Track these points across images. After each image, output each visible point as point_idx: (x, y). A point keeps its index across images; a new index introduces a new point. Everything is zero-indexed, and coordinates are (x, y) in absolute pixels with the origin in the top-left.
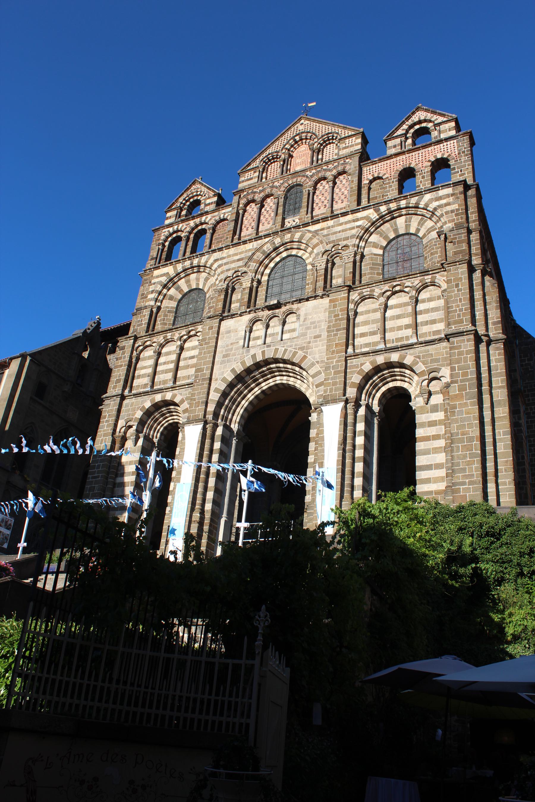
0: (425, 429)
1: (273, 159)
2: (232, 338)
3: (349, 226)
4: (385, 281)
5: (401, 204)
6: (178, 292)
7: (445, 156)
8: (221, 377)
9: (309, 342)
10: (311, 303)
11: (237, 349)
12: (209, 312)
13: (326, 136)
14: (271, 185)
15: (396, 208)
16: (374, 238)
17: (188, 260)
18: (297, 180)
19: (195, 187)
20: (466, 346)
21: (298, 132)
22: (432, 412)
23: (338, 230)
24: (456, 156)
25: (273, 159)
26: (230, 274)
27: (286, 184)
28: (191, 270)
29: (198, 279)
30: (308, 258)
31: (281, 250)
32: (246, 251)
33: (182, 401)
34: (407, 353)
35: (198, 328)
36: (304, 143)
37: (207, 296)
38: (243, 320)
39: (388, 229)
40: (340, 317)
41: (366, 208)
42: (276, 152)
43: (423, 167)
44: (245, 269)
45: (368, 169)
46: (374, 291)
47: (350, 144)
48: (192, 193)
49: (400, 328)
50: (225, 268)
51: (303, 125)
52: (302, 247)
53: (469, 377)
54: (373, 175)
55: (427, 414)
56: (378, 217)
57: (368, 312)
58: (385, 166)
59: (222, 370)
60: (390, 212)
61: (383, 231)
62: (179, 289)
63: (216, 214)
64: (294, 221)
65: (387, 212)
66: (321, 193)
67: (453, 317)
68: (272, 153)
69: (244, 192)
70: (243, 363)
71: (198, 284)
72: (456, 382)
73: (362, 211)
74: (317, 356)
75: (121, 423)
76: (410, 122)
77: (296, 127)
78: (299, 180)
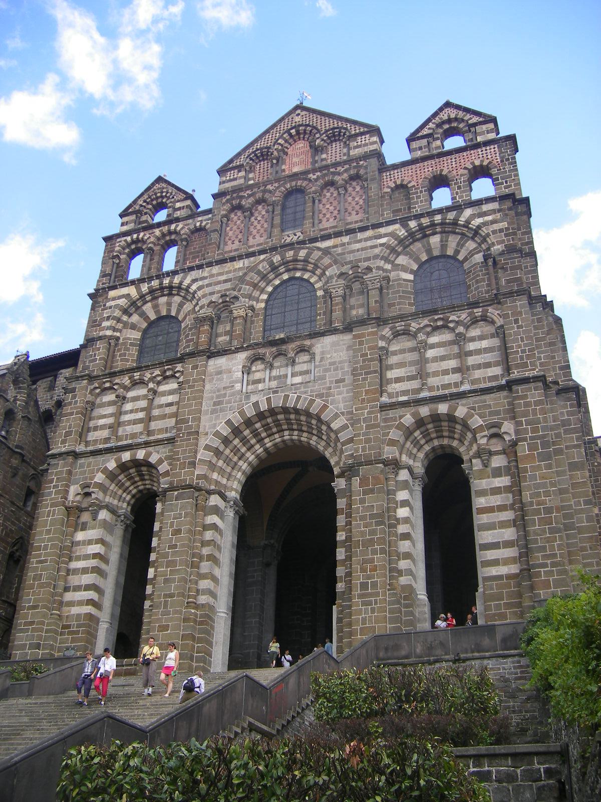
0: (486, 497)
2: (225, 380)
3: (369, 243)
4: (425, 313)
5: (435, 219)
7: (485, 163)
8: (212, 430)
9: (330, 388)
10: (328, 340)
11: (233, 394)
12: (188, 346)
14: (262, 188)
16: (402, 260)
17: (156, 279)
18: (296, 183)
19: (160, 186)
20: (533, 396)
21: (293, 125)
22: (494, 476)
23: (356, 248)
24: (499, 164)
26: (214, 298)
27: (282, 188)
29: (169, 304)
30: (316, 282)
32: (235, 270)
33: (160, 461)
34: (458, 404)
35: (177, 367)
36: (302, 139)
37: (183, 325)
38: (238, 358)
39: (419, 249)
40: (369, 357)
42: (266, 148)
43: (458, 175)
44: (236, 293)
45: (388, 174)
46: (410, 325)
47: (363, 142)
48: (156, 194)
49: (446, 372)
50: (207, 290)
52: (308, 268)
53: (541, 433)
54: (395, 182)
55: (489, 480)
57: (402, 351)
58: (410, 171)
60: (421, 228)
62: (143, 315)
63: (190, 221)
64: (296, 235)
66: (328, 201)
67: (515, 359)
68: (261, 149)
69: (226, 195)
70: (242, 413)
71: (169, 310)
72: (525, 439)
73: (386, 226)
75: (73, 489)
77: (290, 117)
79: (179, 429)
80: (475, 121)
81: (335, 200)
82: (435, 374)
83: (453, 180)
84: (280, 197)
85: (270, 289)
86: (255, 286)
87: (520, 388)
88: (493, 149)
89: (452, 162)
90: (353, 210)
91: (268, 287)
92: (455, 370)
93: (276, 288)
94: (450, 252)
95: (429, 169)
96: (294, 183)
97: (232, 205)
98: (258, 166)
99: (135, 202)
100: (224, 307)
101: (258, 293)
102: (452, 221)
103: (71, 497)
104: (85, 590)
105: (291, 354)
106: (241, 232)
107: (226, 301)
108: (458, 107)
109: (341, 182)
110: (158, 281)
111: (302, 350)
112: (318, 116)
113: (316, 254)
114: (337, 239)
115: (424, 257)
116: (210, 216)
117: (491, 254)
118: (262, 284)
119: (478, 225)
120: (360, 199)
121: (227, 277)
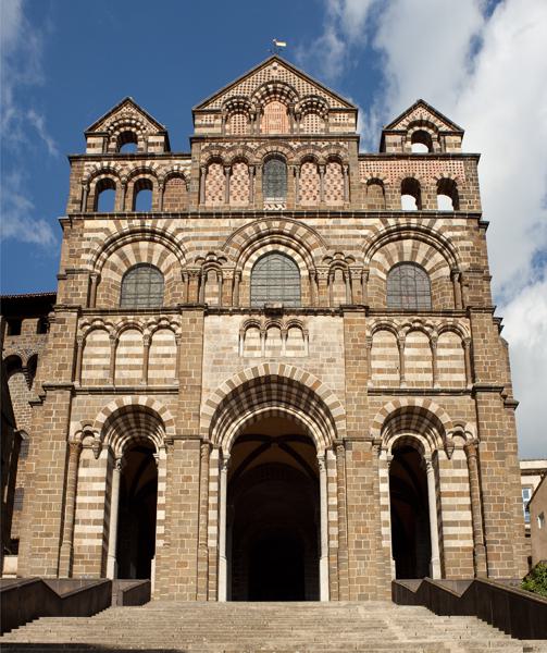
1: (238, 107)
3: (352, 232)
4: (408, 312)
6: (121, 262)
7: (453, 178)
9: (322, 366)
11: (232, 356)
16: (378, 257)
26: (202, 254)
29: (151, 251)
32: (221, 229)
33: (163, 410)
39: (393, 250)
42: (243, 98)
44: (222, 253)
49: (419, 371)
54: (371, 175)
57: (383, 345)
59: (215, 380)
62: (123, 256)
63: (167, 162)
70: (242, 375)
71: (150, 258)
72: (485, 440)
74: (333, 383)
75: (75, 426)
76: (410, 118)
79: (182, 381)
82: (411, 370)
87: (483, 394)
88: (459, 164)
92: (427, 370)
95: (402, 169)
96: (275, 148)
103: (72, 433)
104: (94, 524)
105: (284, 328)
107: (213, 261)
108: (430, 110)
110: (139, 221)
111: (294, 325)
116: (189, 161)
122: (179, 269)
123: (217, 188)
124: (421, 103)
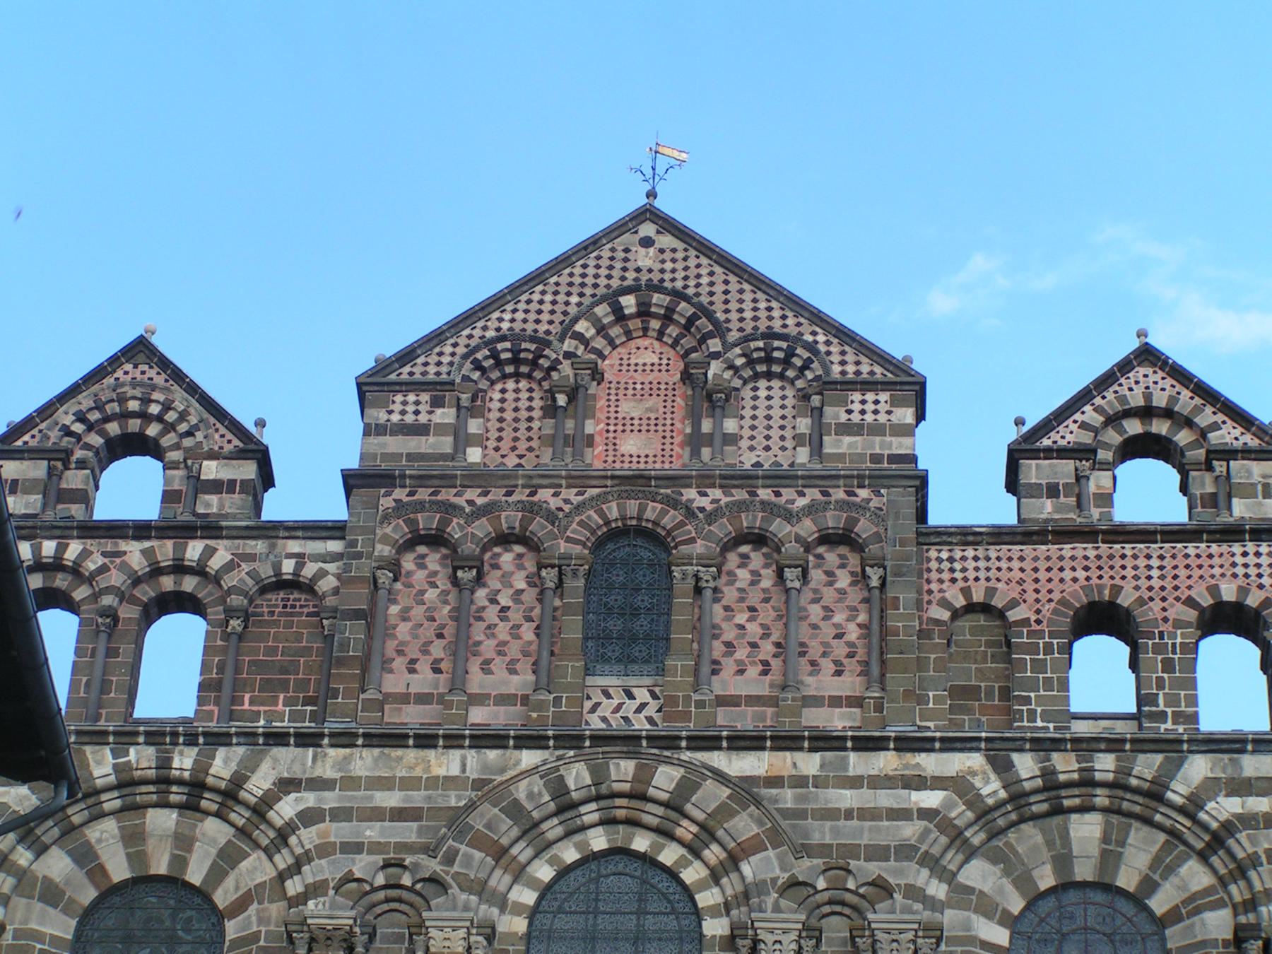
3: (886, 799)
5: (1097, 767)
6: (80, 875)
7: (1253, 601)
13: (761, 344)
14: (520, 495)
15: (1076, 776)
16: (978, 874)
18: (642, 509)
21: (631, 275)
25: (516, 361)
26: (361, 865)
27: (592, 513)
28: (152, 788)
30: (702, 885)
31: (587, 819)
32: (434, 782)
37: (232, 929)
39: (1035, 848)
41: (958, 745)
42: (533, 339)
44: (433, 866)
45: (945, 555)
47: (869, 418)
48: (122, 400)
50: (337, 832)
51: (651, 250)
52: (679, 832)
54: (966, 592)
56: (1003, 794)
60: (1050, 783)
61: (1016, 853)
63: (259, 546)
65: (1039, 782)
66: (742, 600)
68: (515, 337)
73: (942, 750)
76: (1107, 401)
77: (619, 243)
78: (649, 514)
80: (1228, 439)
81: (766, 600)
83: (1150, 636)
84: (584, 545)
85: (545, 873)
86: (500, 853)
89: (1149, 567)
90: (824, 654)
91: (536, 862)
93: (564, 872)
94: (1127, 879)
97: (414, 530)
98: (497, 396)
99: (47, 410)
100: (387, 900)
101: (507, 879)
102: (1146, 786)
106: (440, 636)
108: (1179, 374)
109: (791, 548)
110: (151, 751)
112: (718, 269)
113: (712, 795)
114: (780, 754)
115: (1046, 879)
116: (335, 546)
117: (1256, 927)
118: (522, 852)
119: (1228, 821)
120: (848, 620)
121: (405, 799)
122: (276, 909)
123: (428, 631)
124: (1147, 355)
